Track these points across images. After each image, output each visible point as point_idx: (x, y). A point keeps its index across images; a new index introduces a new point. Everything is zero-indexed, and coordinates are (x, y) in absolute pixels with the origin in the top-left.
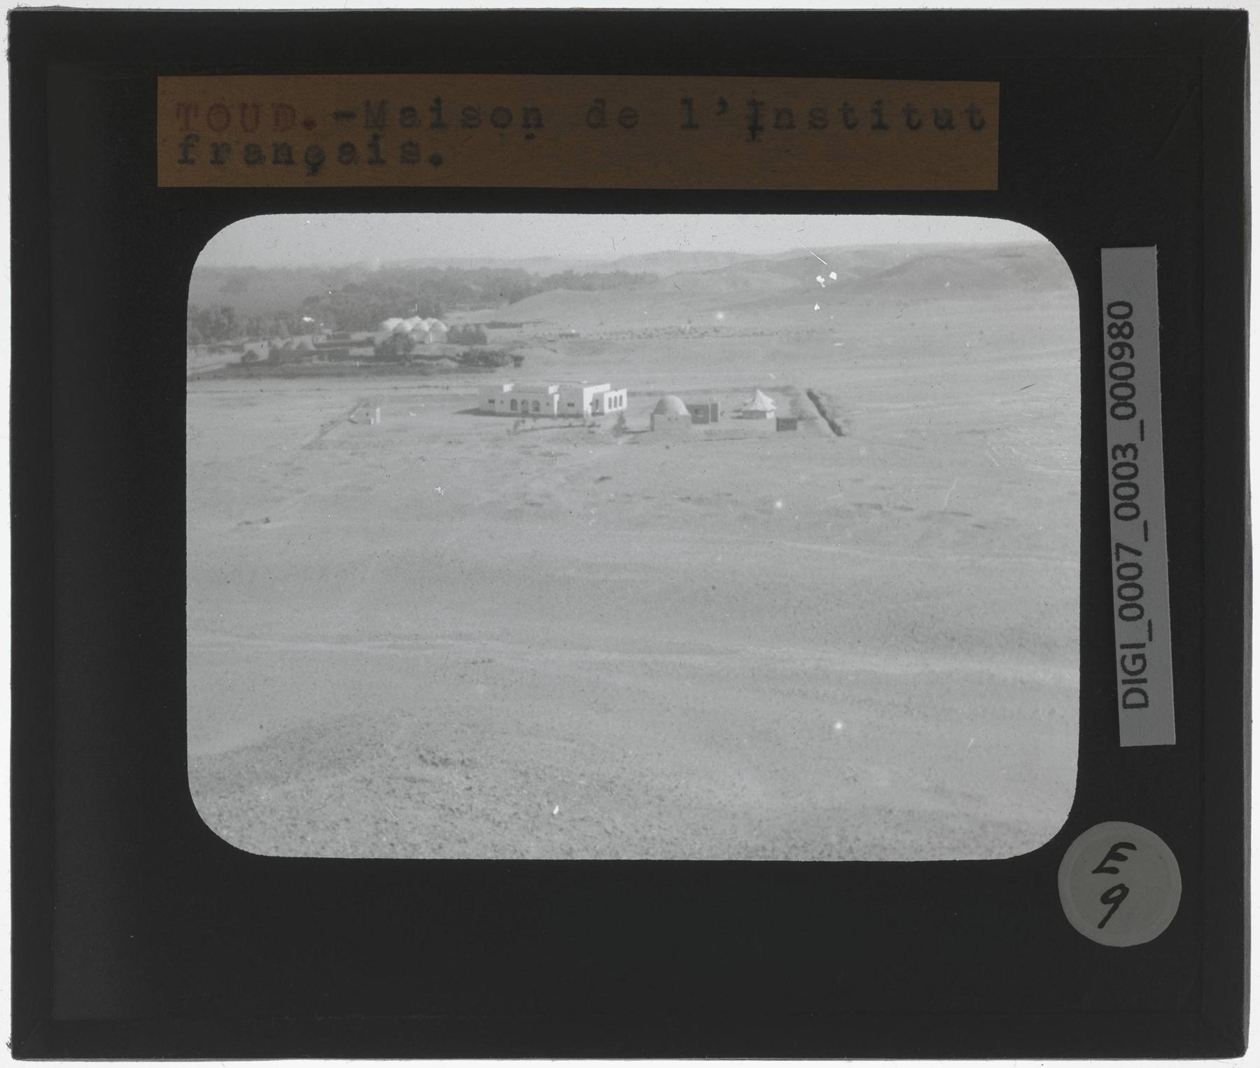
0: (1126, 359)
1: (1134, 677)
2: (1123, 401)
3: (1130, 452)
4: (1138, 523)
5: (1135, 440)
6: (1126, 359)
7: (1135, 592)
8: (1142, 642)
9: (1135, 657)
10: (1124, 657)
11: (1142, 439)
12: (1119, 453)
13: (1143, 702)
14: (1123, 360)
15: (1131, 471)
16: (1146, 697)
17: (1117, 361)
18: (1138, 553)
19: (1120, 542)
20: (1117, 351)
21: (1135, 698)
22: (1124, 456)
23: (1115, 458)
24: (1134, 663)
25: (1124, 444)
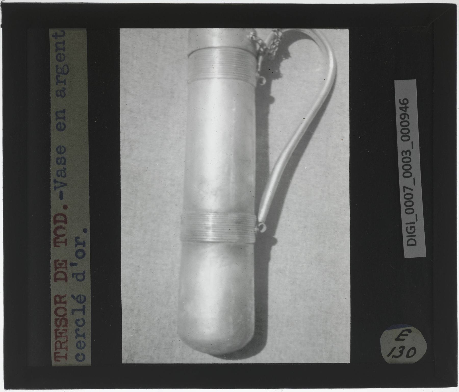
0: (406, 119)
1: (410, 235)
2: (405, 135)
3: (408, 153)
4: (411, 179)
5: (410, 148)
6: (406, 119)
7: (411, 204)
8: (415, 184)
9: (411, 227)
10: (407, 227)
11: (412, 148)
12: (404, 154)
13: (414, 243)
14: (404, 120)
15: (407, 160)
16: (415, 241)
17: (402, 120)
18: (412, 190)
19: (405, 186)
20: (403, 117)
21: (411, 242)
22: (406, 154)
23: (403, 155)
24: (411, 229)
25: (406, 150)
